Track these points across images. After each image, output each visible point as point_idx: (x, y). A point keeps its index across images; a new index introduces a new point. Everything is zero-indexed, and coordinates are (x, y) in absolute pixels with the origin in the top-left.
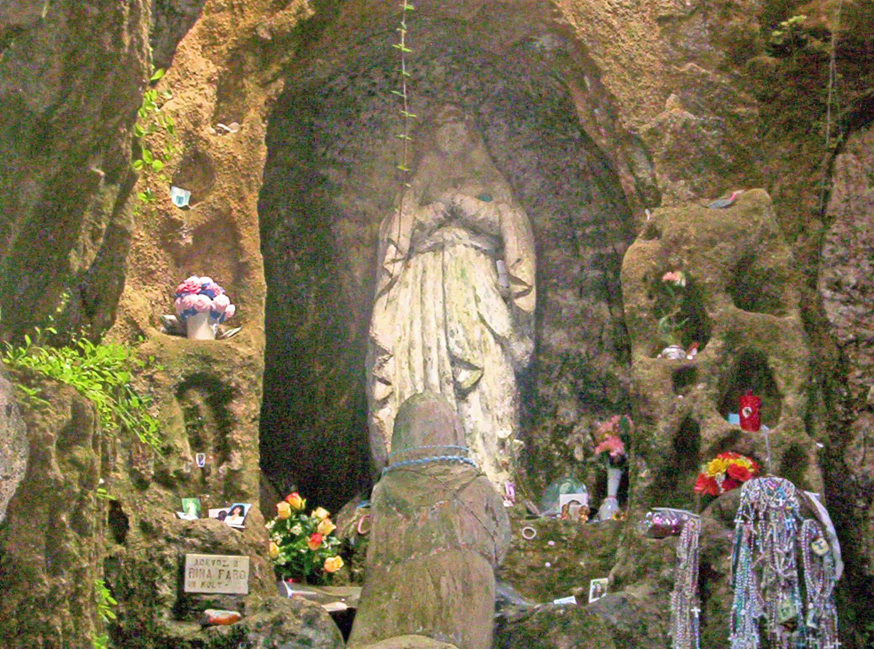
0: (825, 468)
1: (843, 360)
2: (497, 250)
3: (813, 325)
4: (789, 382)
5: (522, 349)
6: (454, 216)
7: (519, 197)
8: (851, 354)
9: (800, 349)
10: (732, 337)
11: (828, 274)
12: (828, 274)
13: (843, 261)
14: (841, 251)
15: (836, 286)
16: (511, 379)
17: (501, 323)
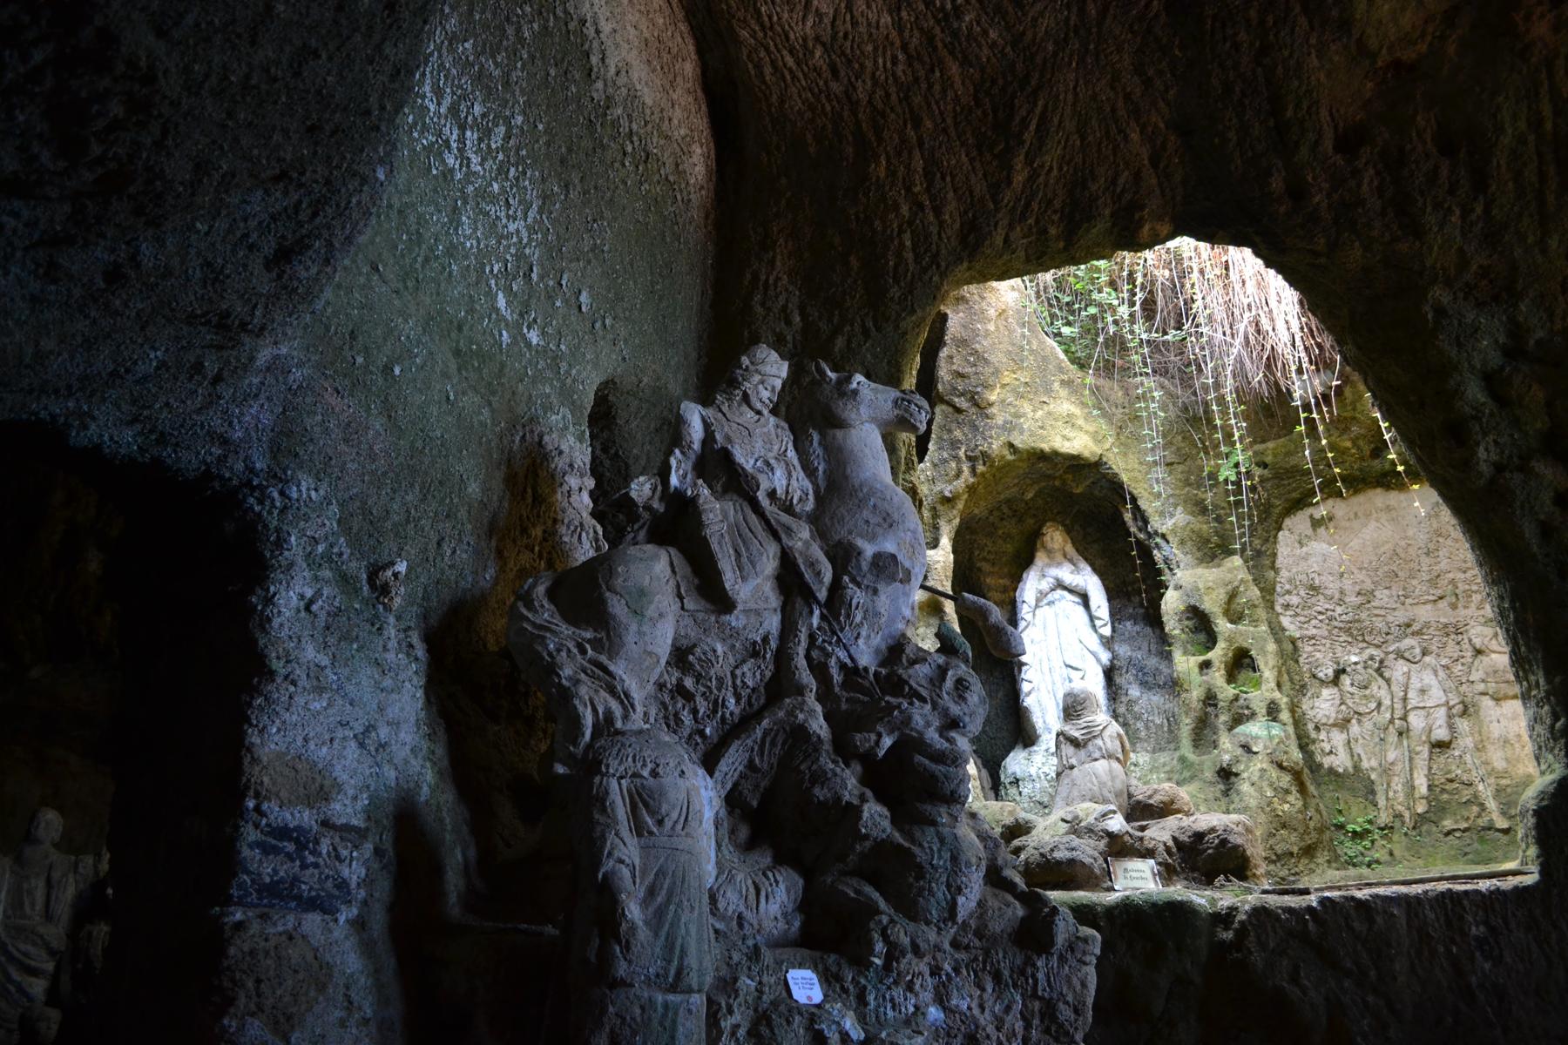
0: (1292, 711)
1: (1296, 649)
2: (1085, 599)
3: (1277, 631)
4: (1266, 663)
5: (1105, 657)
6: (1060, 585)
7: (1096, 570)
8: (1299, 644)
9: (1272, 647)
10: (1230, 640)
11: (1281, 600)
12: (1281, 600)
13: (1289, 592)
14: (1287, 587)
15: (1287, 606)
16: (1101, 675)
17: (1094, 643)
